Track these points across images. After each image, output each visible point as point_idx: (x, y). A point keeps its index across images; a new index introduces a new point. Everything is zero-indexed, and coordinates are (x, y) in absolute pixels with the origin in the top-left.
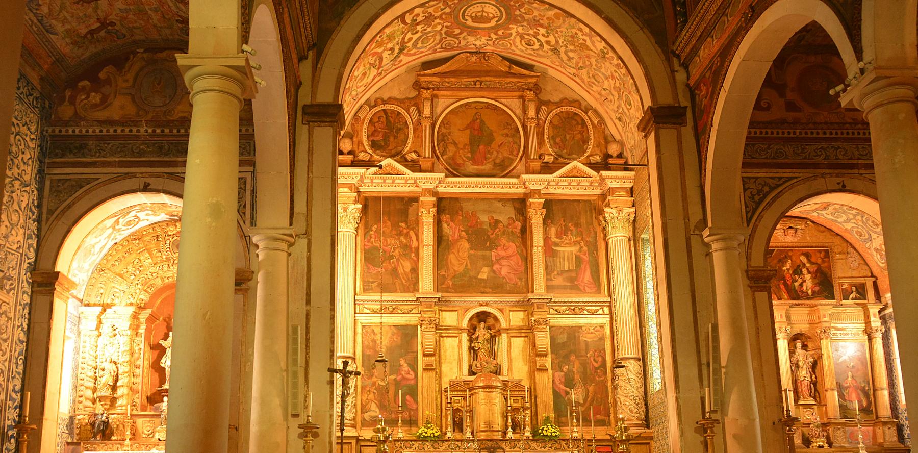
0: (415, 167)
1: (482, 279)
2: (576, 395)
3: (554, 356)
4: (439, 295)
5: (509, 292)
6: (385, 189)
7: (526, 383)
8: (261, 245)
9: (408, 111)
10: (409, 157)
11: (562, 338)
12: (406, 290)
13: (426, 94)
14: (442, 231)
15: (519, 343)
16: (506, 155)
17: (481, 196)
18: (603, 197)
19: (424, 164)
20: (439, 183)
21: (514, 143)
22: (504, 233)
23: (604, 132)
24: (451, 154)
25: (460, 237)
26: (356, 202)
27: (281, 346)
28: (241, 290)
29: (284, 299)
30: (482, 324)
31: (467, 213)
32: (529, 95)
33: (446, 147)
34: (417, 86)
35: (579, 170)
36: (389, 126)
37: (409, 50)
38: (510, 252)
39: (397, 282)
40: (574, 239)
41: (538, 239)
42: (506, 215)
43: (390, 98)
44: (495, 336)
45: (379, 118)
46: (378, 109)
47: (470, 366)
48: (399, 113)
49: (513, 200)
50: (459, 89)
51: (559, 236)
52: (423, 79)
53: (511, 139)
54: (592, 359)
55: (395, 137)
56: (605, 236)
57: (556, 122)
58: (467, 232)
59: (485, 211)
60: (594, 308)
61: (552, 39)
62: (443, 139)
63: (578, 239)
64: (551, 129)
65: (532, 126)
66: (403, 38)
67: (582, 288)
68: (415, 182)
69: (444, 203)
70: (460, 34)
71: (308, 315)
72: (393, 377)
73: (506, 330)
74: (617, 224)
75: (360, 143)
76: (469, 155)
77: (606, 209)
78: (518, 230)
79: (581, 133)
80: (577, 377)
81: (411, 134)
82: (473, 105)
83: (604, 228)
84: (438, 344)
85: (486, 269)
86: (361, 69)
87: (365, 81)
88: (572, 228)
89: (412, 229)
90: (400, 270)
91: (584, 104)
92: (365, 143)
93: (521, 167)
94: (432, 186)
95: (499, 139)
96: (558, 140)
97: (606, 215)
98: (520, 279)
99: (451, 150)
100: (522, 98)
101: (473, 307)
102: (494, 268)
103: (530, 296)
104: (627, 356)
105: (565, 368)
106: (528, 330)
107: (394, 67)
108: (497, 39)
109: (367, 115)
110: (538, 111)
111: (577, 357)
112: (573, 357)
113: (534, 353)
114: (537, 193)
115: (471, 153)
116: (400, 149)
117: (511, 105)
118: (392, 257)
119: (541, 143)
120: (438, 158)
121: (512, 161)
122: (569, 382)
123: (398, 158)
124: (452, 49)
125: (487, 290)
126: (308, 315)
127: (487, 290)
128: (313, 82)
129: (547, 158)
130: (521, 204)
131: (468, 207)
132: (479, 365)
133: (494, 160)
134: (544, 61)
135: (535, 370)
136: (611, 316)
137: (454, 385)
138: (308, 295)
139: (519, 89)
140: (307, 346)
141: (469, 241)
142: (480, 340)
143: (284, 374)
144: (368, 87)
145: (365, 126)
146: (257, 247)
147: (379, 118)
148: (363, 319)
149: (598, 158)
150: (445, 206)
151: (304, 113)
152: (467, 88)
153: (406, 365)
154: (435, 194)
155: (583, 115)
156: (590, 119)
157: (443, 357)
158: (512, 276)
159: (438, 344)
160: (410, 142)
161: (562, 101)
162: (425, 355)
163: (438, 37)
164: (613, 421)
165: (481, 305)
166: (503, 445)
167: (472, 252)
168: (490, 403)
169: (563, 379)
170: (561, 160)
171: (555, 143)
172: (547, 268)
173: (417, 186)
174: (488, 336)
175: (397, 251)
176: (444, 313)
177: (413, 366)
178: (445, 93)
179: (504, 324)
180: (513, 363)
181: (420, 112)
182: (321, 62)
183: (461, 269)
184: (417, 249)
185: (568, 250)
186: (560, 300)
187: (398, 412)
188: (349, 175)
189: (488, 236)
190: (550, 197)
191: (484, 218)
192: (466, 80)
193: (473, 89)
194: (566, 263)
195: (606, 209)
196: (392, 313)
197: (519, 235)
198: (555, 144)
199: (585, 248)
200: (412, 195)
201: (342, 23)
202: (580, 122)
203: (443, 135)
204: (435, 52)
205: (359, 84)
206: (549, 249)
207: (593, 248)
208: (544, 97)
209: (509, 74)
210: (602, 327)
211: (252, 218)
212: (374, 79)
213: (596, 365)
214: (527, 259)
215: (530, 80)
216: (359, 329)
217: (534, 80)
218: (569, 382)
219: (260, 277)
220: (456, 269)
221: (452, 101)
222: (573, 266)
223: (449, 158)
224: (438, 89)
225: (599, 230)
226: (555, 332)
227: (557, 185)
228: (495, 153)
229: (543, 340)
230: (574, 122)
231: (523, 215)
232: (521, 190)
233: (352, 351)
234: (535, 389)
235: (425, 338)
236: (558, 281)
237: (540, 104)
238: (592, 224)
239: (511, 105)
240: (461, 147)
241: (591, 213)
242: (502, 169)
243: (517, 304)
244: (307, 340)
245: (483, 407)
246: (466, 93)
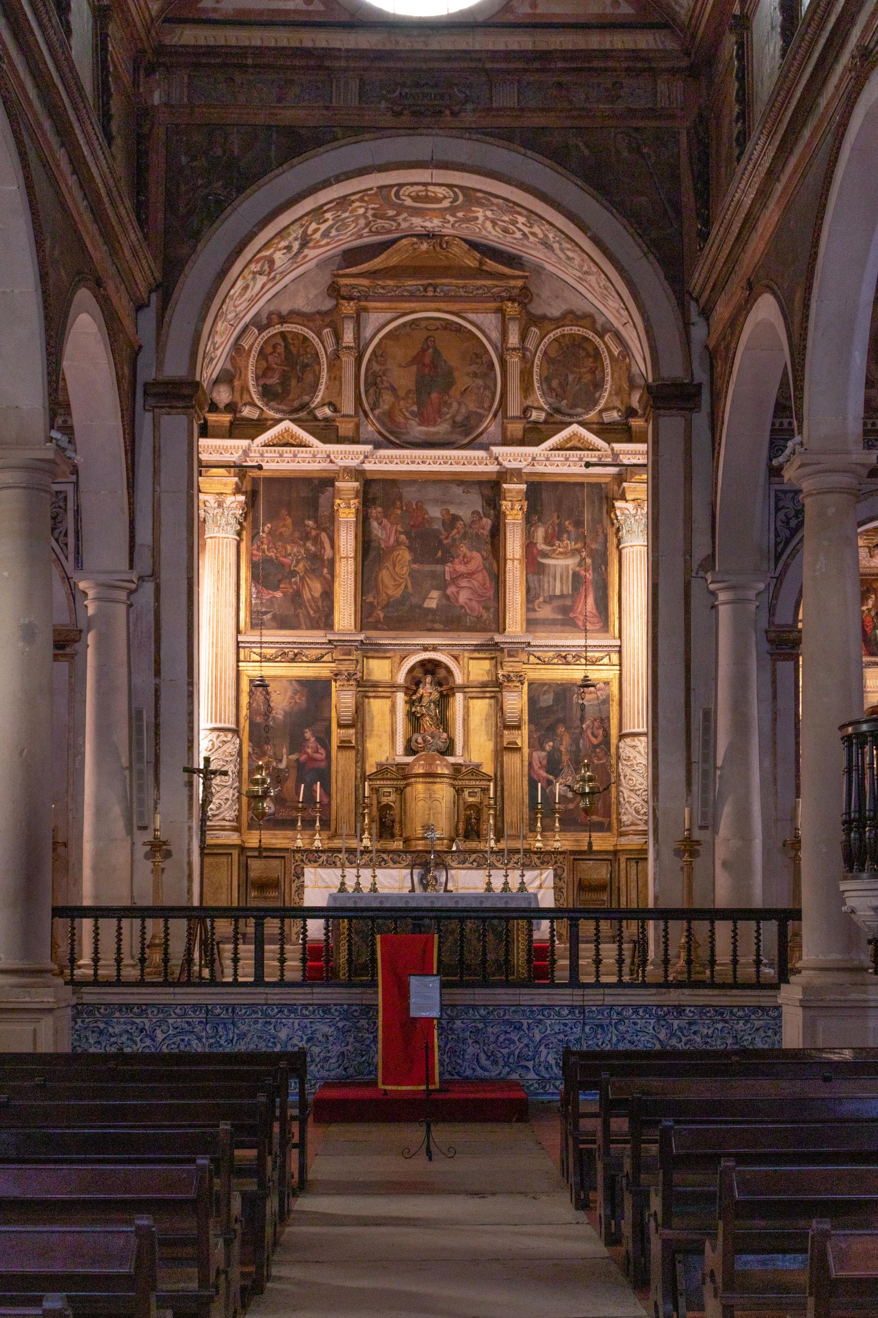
0: (327, 432)
1: (429, 610)
3: (532, 726)
4: (361, 637)
6: (283, 466)
7: (488, 769)
8: (91, 594)
9: (319, 335)
10: (319, 414)
11: (547, 700)
12: (314, 625)
13: (348, 308)
14: (370, 532)
15: (481, 707)
16: (472, 407)
17: (431, 477)
18: (620, 479)
19: (345, 428)
20: (366, 457)
21: (487, 387)
22: (464, 536)
23: (629, 369)
24: (386, 407)
25: (398, 543)
26: (238, 491)
27: (121, 734)
28: (64, 655)
29: (124, 670)
30: (429, 679)
31: (409, 504)
32: (512, 308)
33: (378, 395)
34: (334, 291)
35: (581, 439)
36: (290, 359)
37: (318, 242)
38: (472, 566)
39: (301, 612)
40: (571, 545)
41: (514, 546)
42: (468, 507)
43: (292, 313)
44: (447, 696)
45: (275, 347)
46: (272, 331)
47: (409, 741)
48: (305, 339)
49: (480, 483)
50: (401, 298)
51: (548, 541)
52: (343, 281)
53: (480, 382)
54: (589, 733)
55: (300, 380)
56: (619, 543)
57: (553, 354)
58: (407, 534)
59: (436, 501)
60: (597, 655)
61: (536, 229)
62: (374, 382)
63: (579, 545)
64: (545, 365)
65: (514, 360)
66: (305, 233)
67: (580, 623)
68: (328, 456)
69: (375, 490)
70: (398, 214)
71: (157, 691)
72: (294, 757)
73: (462, 688)
74: (635, 528)
75: (245, 389)
76: (415, 408)
77: (619, 504)
78: (486, 532)
79: (592, 372)
80: (565, 758)
81: (324, 374)
82: (424, 324)
83: (618, 530)
84: (359, 709)
85: (435, 594)
86: (240, 284)
87: (248, 295)
88: (570, 528)
89: (325, 530)
90: (306, 595)
91: (600, 320)
92: (252, 390)
94: (353, 463)
95: (462, 381)
96: (555, 383)
97: (618, 513)
98: (487, 609)
99: (387, 399)
100: (500, 311)
101: (415, 652)
102: (448, 592)
103: (498, 638)
104: (636, 730)
105: (549, 745)
106: (494, 689)
107: (295, 266)
108: (456, 222)
109: (254, 341)
110: (523, 337)
111: (567, 729)
112: (561, 729)
113: (502, 724)
114: (517, 474)
115: (419, 404)
116: (306, 398)
117: (484, 323)
118: (294, 574)
119: (527, 389)
120: (366, 415)
121: (481, 418)
122: (553, 767)
123: (302, 414)
124: (389, 232)
125: (437, 626)
126: (157, 691)
127: (437, 626)
128: (158, 334)
129: (535, 415)
130: (491, 488)
131: (410, 494)
132: (420, 740)
133: (453, 417)
134: (534, 253)
136: (620, 665)
137: (383, 770)
138: (157, 662)
139: (494, 298)
140: (157, 735)
141: (410, 548)
142: (425, 701)
143: (127, 773)
144: (253, 301)
145: (252, 361)
146: (86, 594)
147: (275, 347)
148: (252, 670)
149: (615, 415)
150: (375, 492)
151: (145, 393)
152: (412, 297)
153: (313, 739)
154: (358, 474)
155: (597, 340)
156: (608, 346)
157: (368, 727)
158: (474, 604)
159: (359, 709)
160: (322, 387)
161: (564, 316)
162: (340, 726)
163: (362, 222)
164: (614, 822)
165: (425, 648)
166: (448, 859)
167: (416, 566)
168: (430, 797)
169: (545, 762)
170: (558, 417)
171: (551, 389)
172: (528, 591)
173: (331, 462)
174: (436, 695)
175: (301, 565)
176: (371, 660)
177: (324, 740)
178: (379, 305)
179: (459, 679)
180: (472, 738)
181: (338, 337)
182: (169, 312)
183: (397, 593)
184: (332, 563)
185: (562, 564)
186: (543, 642)
187: (297, 809)
188: (226, 449)
189: (440, 542)
190: (536, 479)
191: (435, 512)
192: (411, 283)
193: (424, 298)
194: (558, 584)
195: (619, 504)
196: (293, 660)
197: (489, 539)
198: (549, 391)
199: (589, 561)
200: (324, 475)
201: (199, 248)
202: (592, 352)
203: (375, 375)
204: (361, 236)
205: (238, 303)
206: (533, 564)
207: (601, 561)
208: (537, 309)
209: (480, 272)
210: (607, 683)
211: (77, 552)
212: (262, 288)
213: (595, 741)
214: (498, 579)
215: (513, 283)
216: (245, 686)
217: (520, 283)
219: (91, 638)
220: (390, 592)
221: (389, 316)
222: (568, 589)
223: (384, 414)
224: (367, 298)
225: (611, 531)
227: (545, 459)
228: (455, 405)
229: (516, 702)
230: (582, 353)
231: (495, 508)
232: (493, 468)
233: (233, 719)
234: (502, 778)
235: (343, 700)
236: (545, 612)
237: (531, 320)
238: (601, 521)
239: (484, 323)
240: (402, 393)
241: (601, 503)
242: (466, 435)
244: (157, 726)
245: (421, 803)
246: (413, 305)
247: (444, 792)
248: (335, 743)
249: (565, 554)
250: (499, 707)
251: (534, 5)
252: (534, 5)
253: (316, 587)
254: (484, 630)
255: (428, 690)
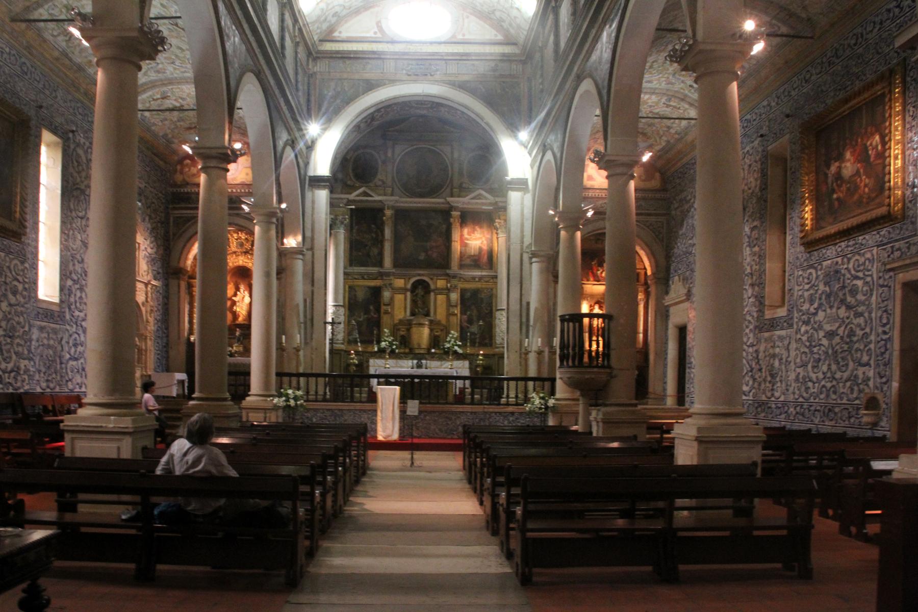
2: (474, 329)
5: (437, 268)
12: (374, 265)
35: (480, 195)
51: (469, 234)
73: (433, 291)
78: (444, 230)
84: (392, 299)
90: (371, 254)
93: (448, 190)
94: (391, 204)
103: (448, 271)
114: (456, 209)
122: (470, 321)
135: (449, 315)
137: (401, 322)
148: (350, 283)
154: (393, 208)
165: (419, 275)
177: (378, 310)
179: (432, 287)
181: (385, 154)
191: (423, 222)
199: (485, 242)
218: (470, 321)
226: (463, 292)
235: (386, 294)
243: (441, 275)
247: (426, 331)
248: (382, 311)
249: (476, 239)
250: (448, 299)
251: (464, 35)
252: (464, 35)
253: (375, 251)
254: (442, 268)
255: (420, 291)
